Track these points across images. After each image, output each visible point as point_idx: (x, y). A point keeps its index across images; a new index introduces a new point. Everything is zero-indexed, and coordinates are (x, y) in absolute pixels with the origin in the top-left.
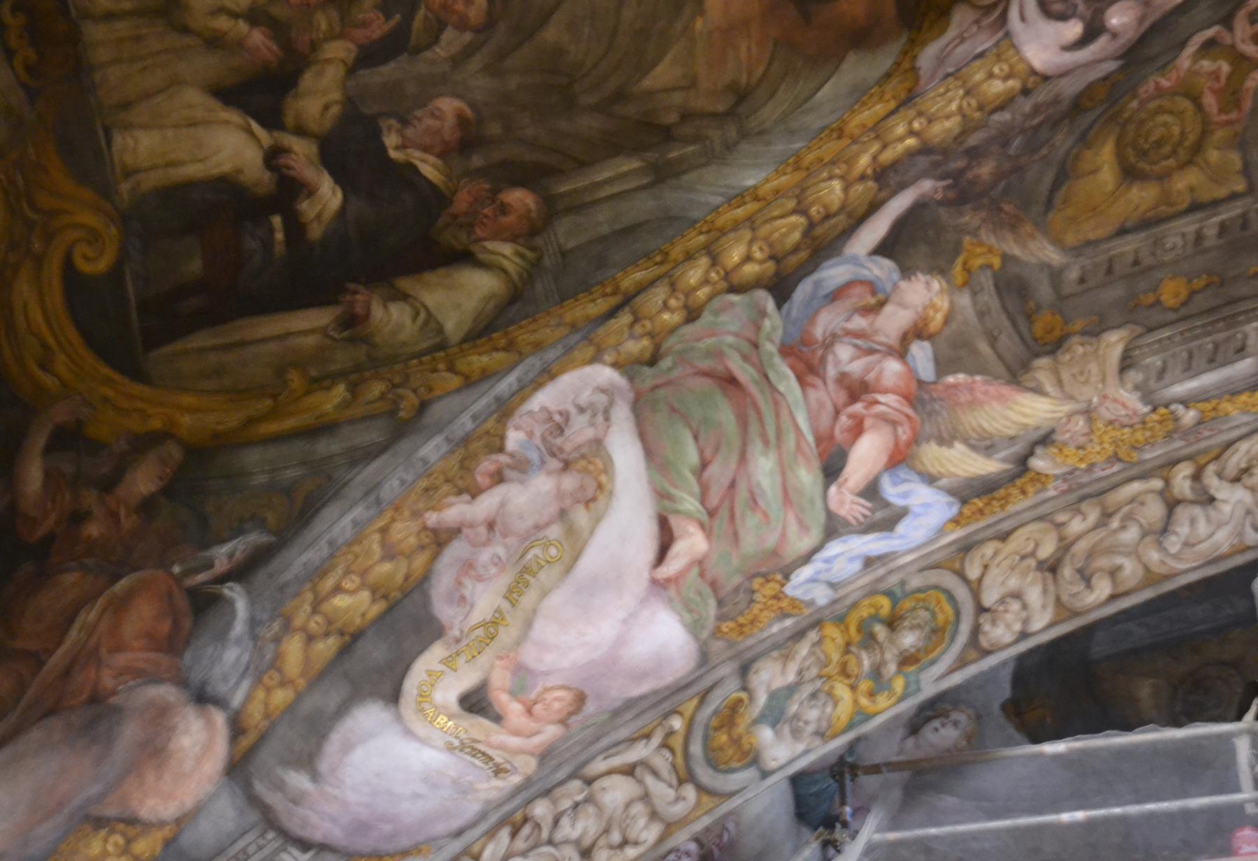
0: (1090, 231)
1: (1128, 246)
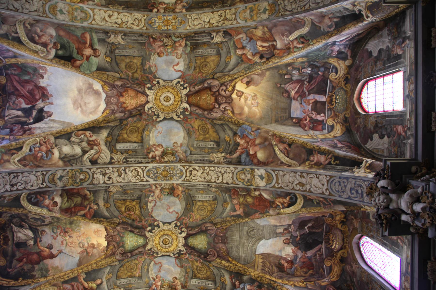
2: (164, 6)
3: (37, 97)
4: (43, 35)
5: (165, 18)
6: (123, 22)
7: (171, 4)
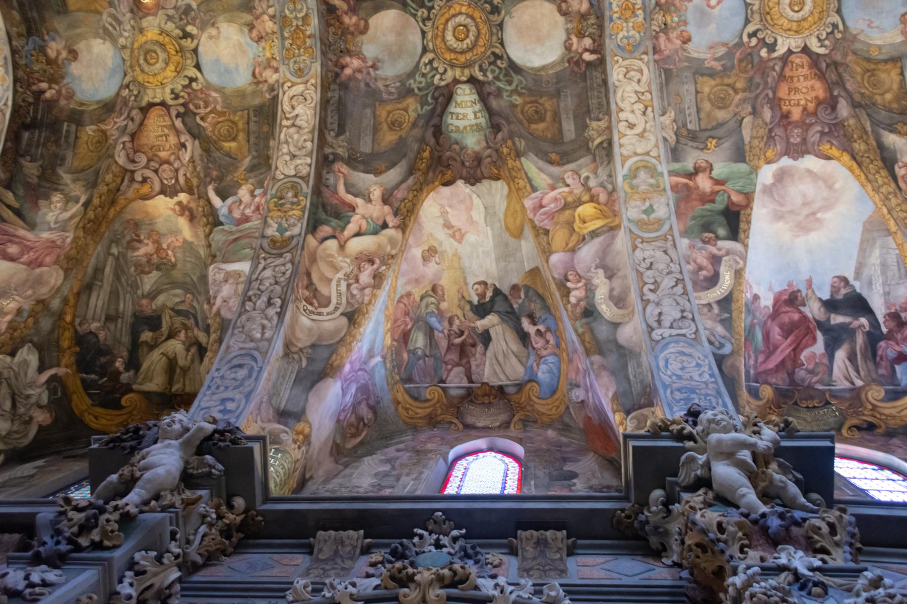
0: (245, 149)
1: (252, 139)
2: (574, 40)
3: (796, 316)
4: (695, 262)
5: (615, 16)
6: (639, 100)
7: (570, 26)
